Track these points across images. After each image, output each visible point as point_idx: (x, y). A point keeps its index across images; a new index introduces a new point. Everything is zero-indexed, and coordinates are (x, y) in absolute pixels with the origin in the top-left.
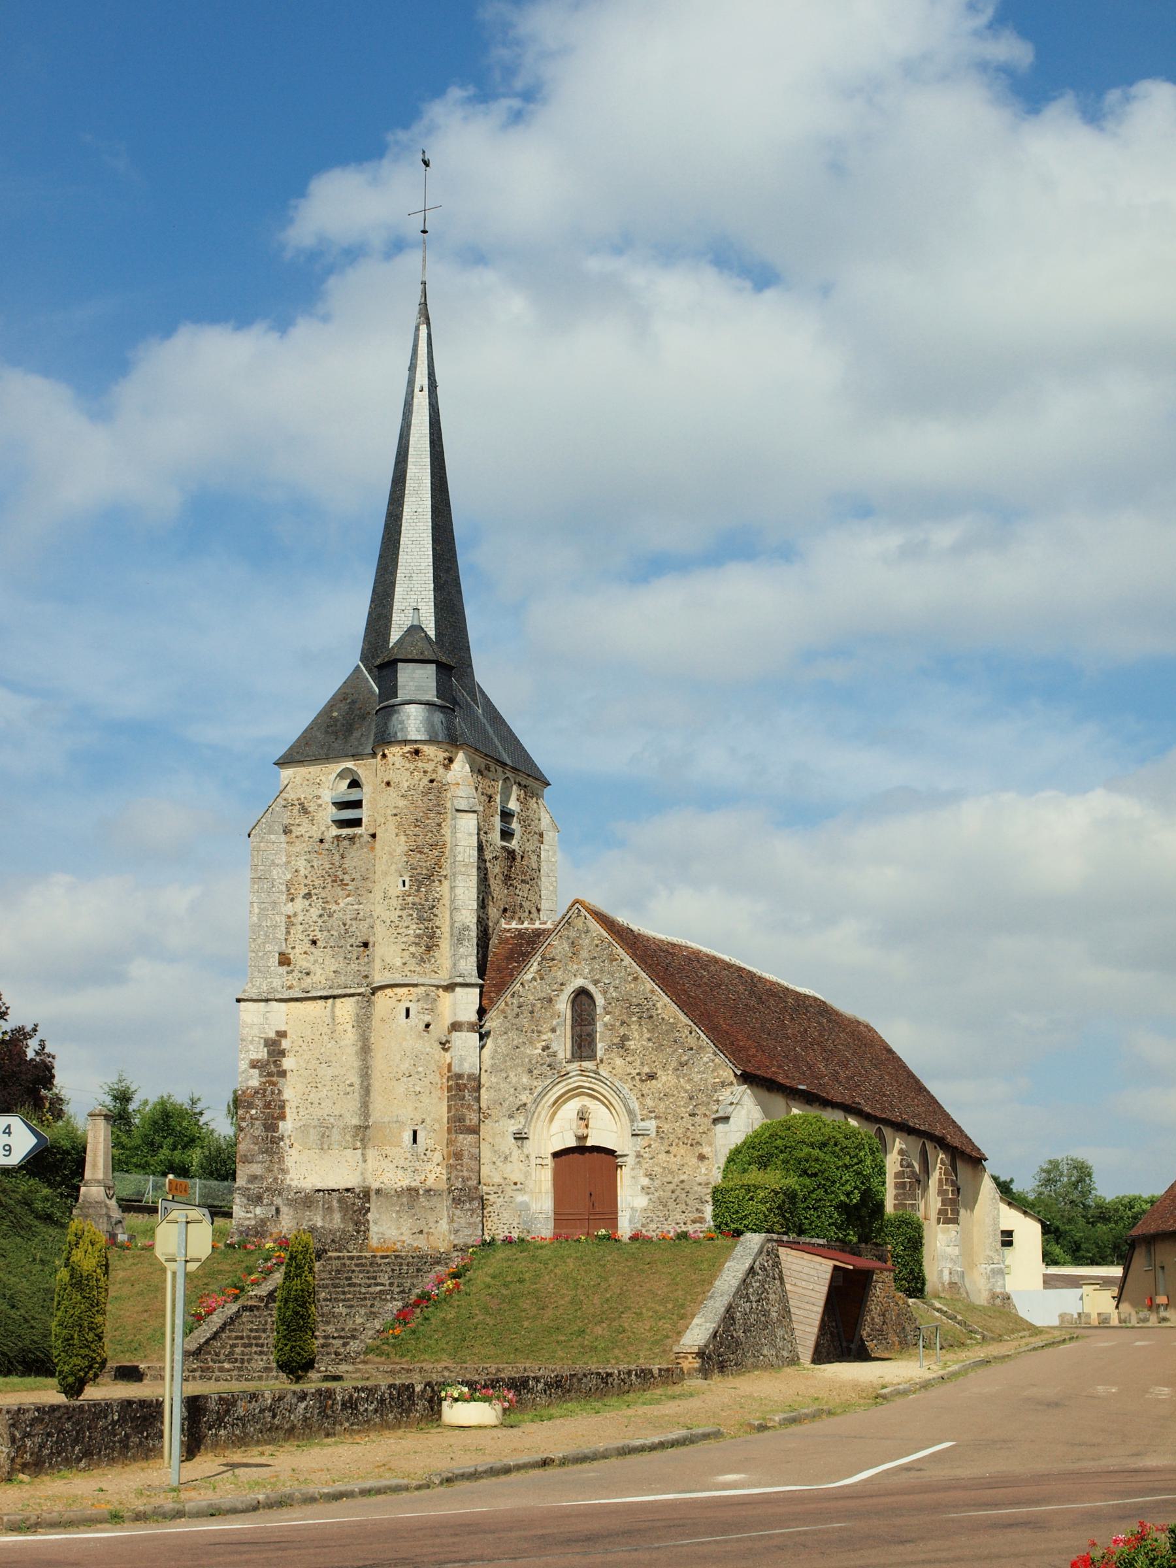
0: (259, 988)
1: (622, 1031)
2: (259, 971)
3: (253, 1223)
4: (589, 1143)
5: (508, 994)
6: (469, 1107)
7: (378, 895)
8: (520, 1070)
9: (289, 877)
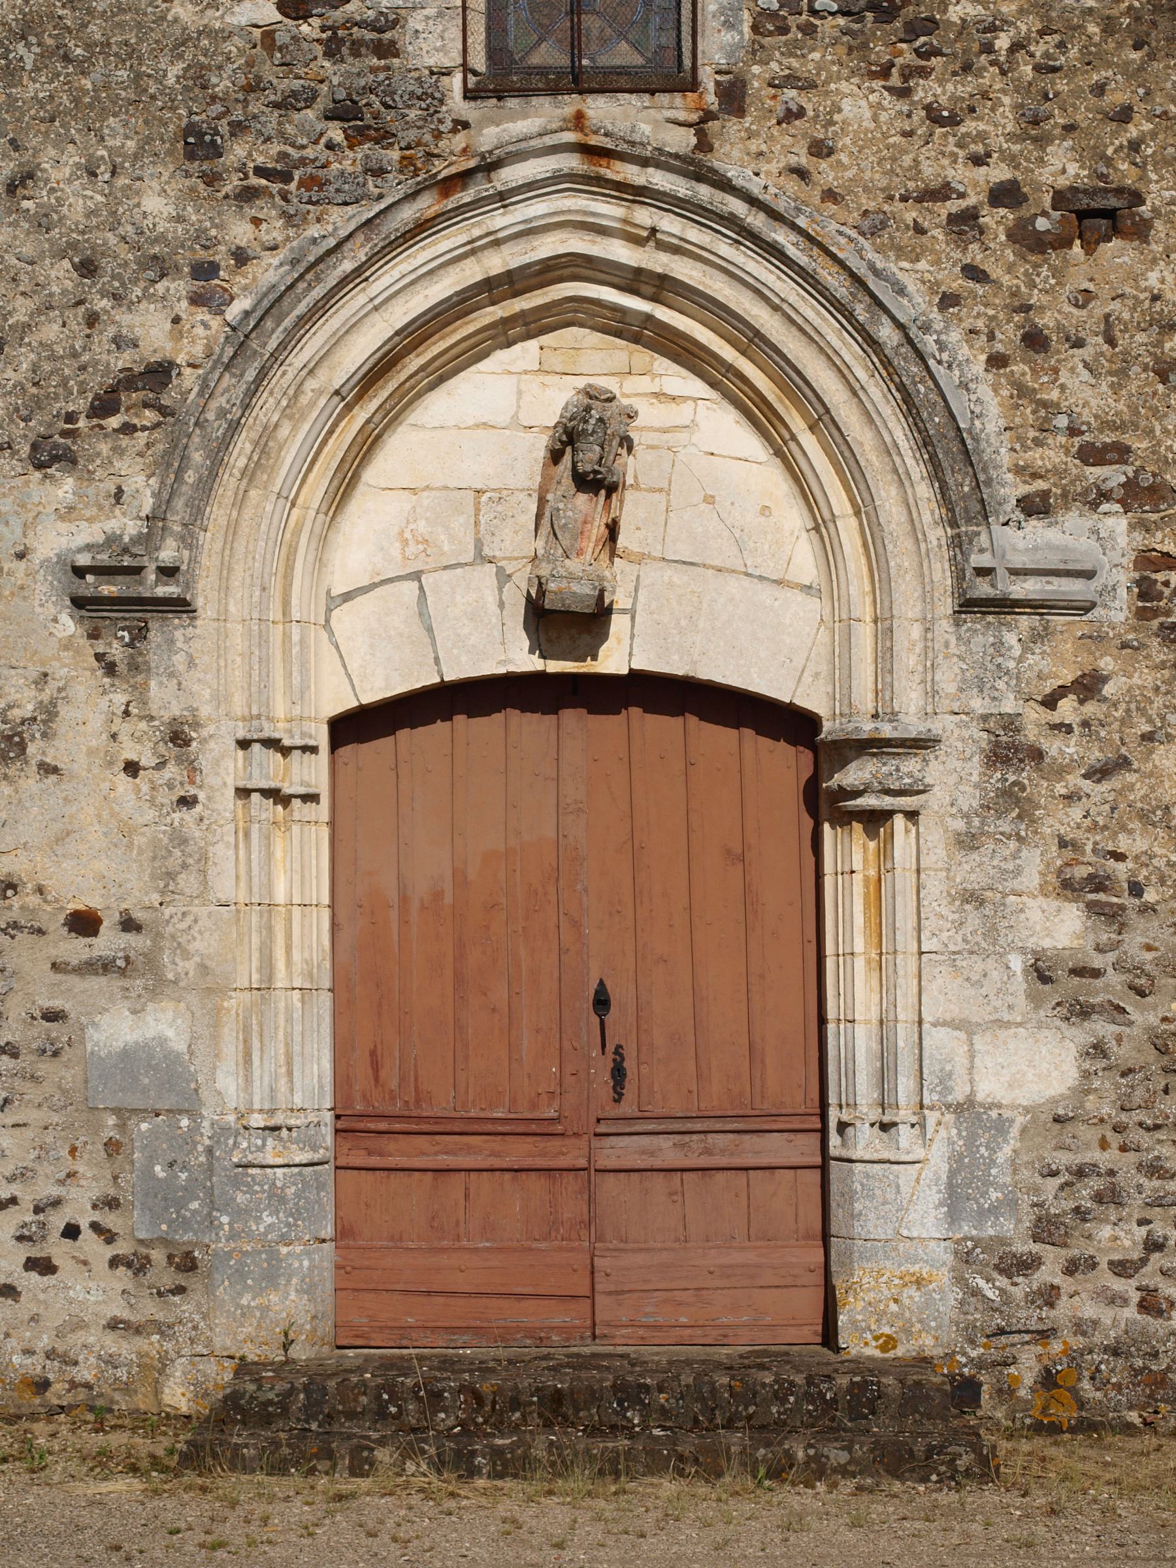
4: (612, 659)
8: (120, 136)
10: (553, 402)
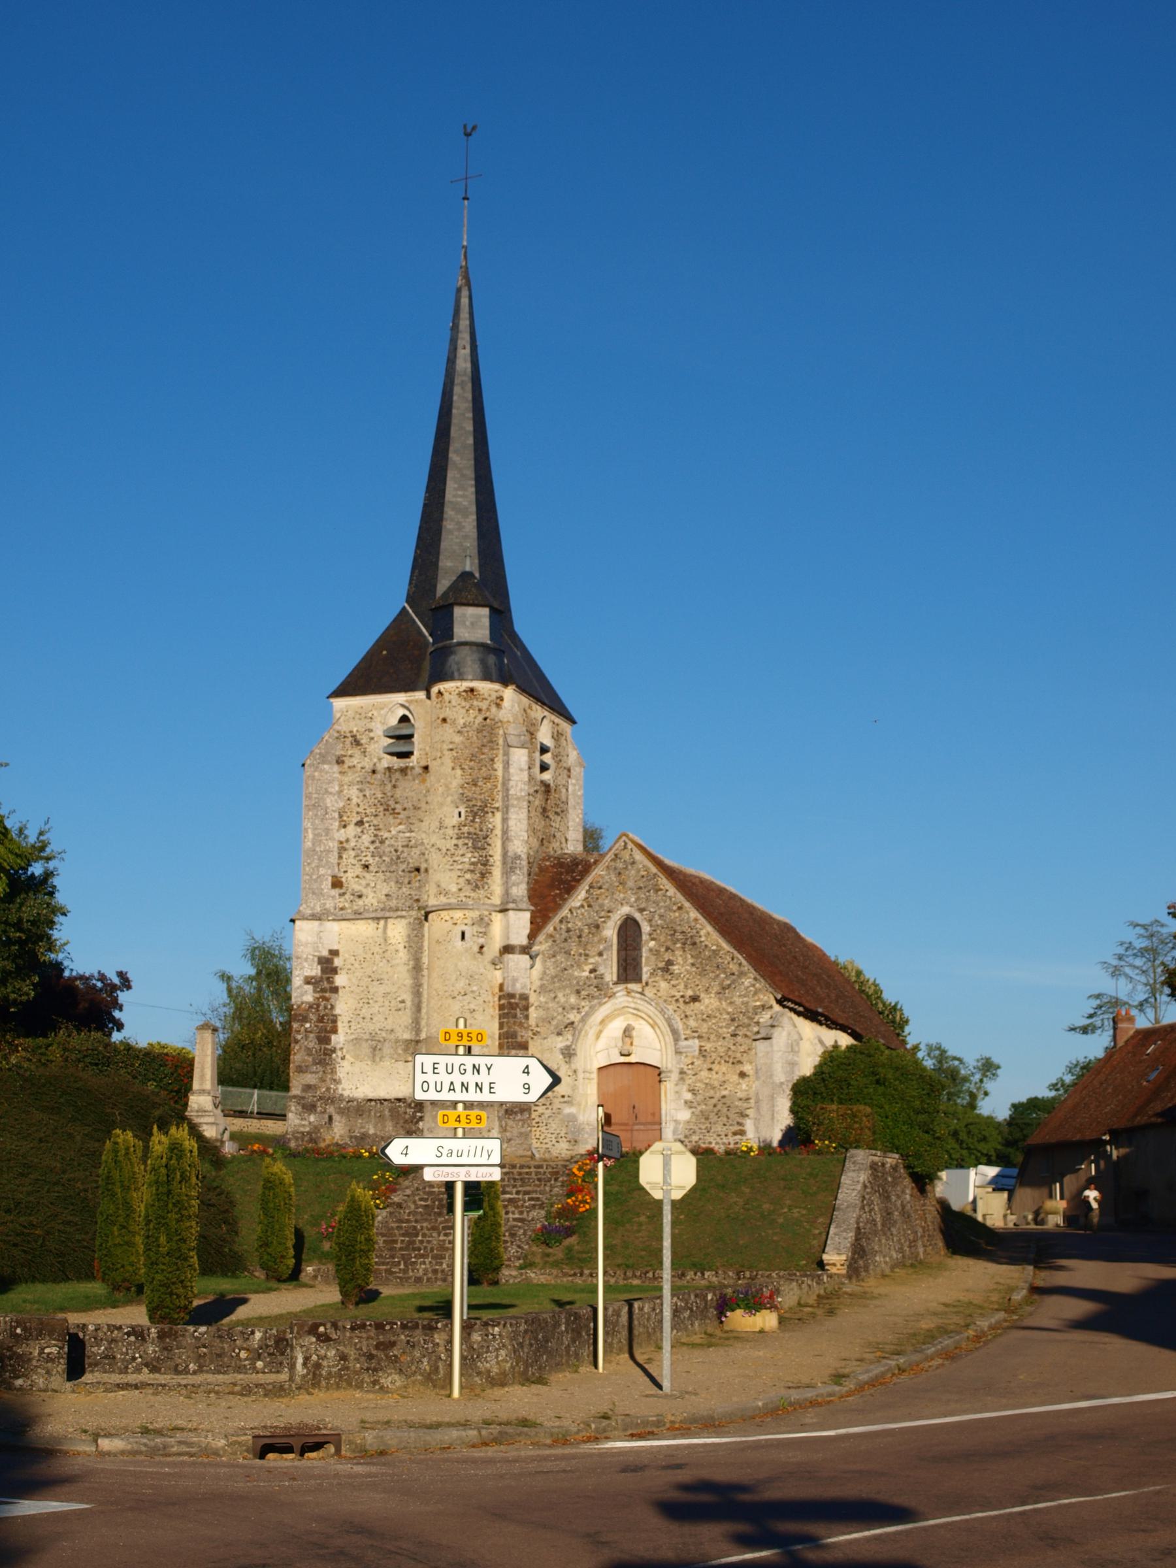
0: (313, 909)
1: (667, 956)
2: (314, 893)
3: (307, 1129)
4: (632, 1059)
5: (557, 919)
6: (521, 1025)
7: (430, 823)
8: (568, 991)
9: (341, 804)
10: (624, 1025)
